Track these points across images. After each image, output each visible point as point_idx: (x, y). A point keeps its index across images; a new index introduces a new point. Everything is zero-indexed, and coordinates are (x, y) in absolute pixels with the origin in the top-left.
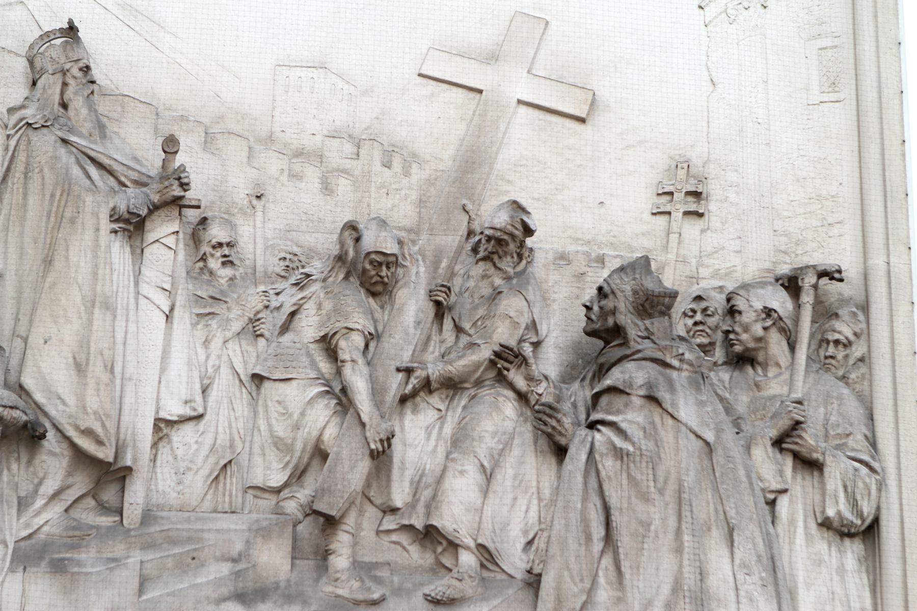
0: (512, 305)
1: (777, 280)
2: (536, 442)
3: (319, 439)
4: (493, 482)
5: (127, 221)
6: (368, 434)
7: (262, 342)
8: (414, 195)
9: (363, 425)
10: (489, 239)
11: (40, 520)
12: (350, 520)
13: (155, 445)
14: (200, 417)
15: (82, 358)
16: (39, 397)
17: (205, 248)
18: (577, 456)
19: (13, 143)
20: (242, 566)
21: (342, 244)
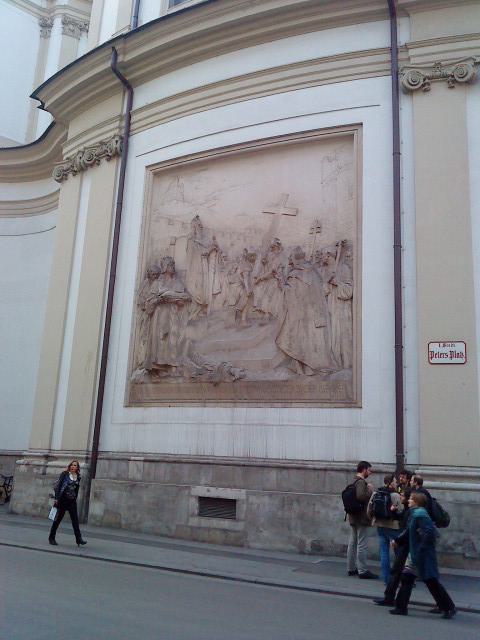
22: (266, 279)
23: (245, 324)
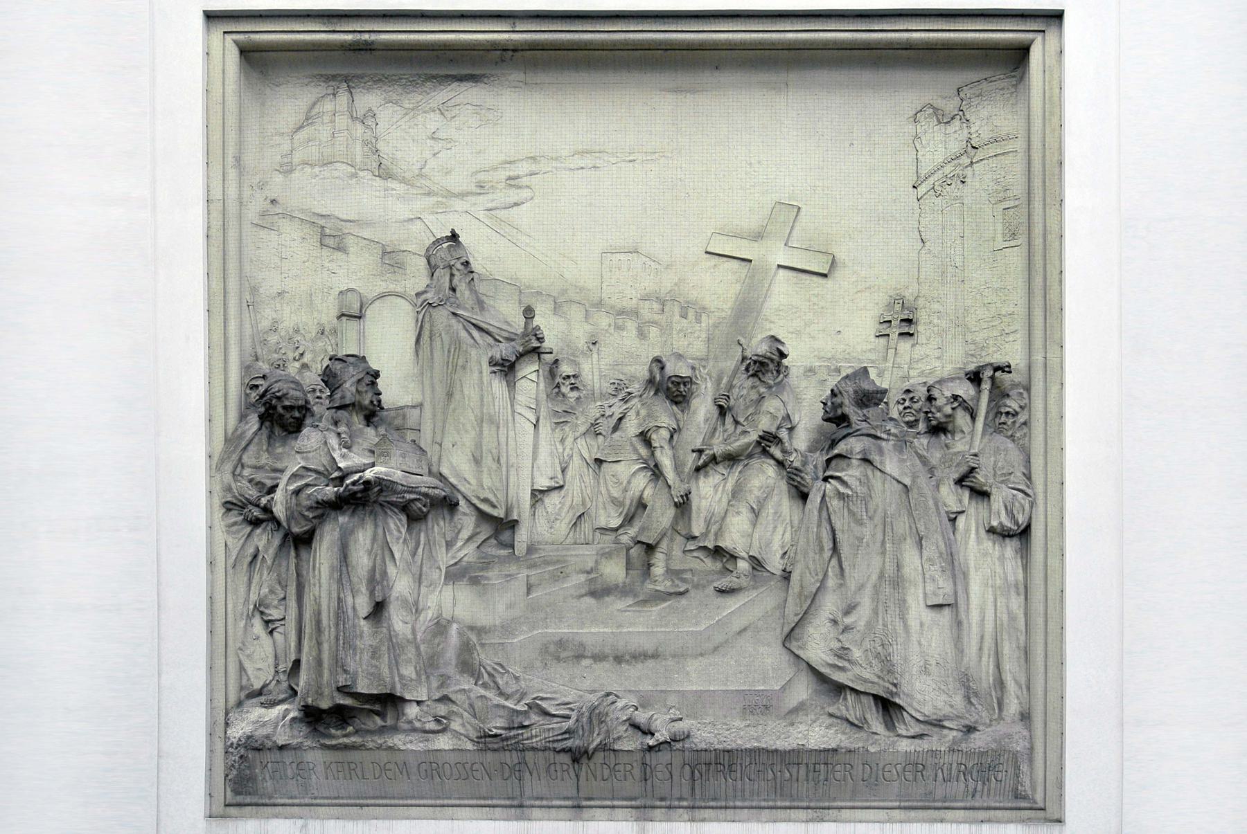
0: (772, 405)
1: (966, 375)
2: (789, 492)
3: (641, 497)
4: (760, 517)
5: (502, 365)
6: (673, 492)
7: (600, 437)
8: (704, 336)
9: (670, 487)
10: (755, 362)
11: (461, 554)
12: (664, 545)
13: (533, 506)
14: (561, 487)
15: (478, 454)
16: (452, 480)
17: (558, 380)
18: (815, 499)
21: (651, 371)
22: (732, 459)
23: (664, 585)
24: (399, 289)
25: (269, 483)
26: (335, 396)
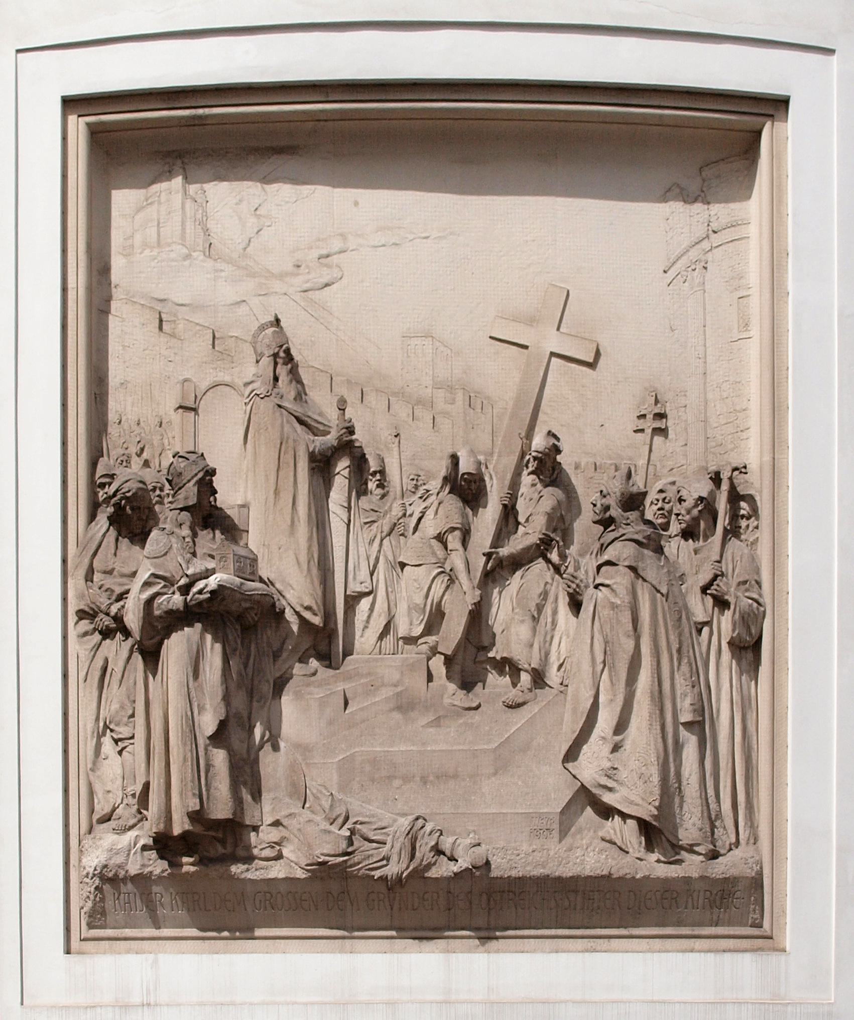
3: (439, 604)
5: (319, 461)
19: (249, 407)
20: (399, 689)
24: (227, 379)
25: (118, 590)
26: (179, 497)
